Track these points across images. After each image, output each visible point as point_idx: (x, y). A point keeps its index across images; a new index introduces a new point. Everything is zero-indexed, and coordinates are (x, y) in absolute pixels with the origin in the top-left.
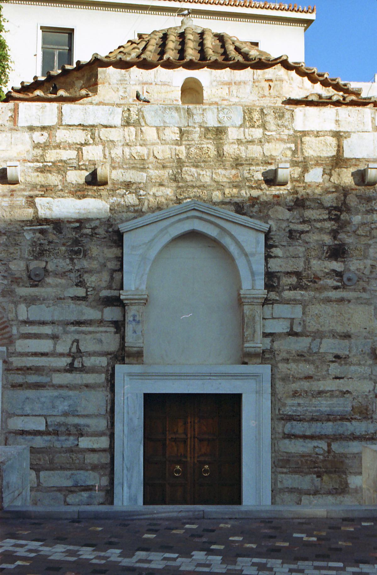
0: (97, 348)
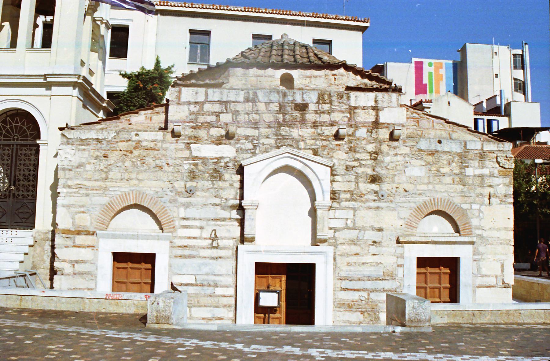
0: (227, 235)
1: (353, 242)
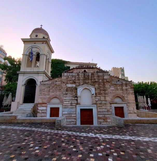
0: (74, 103)
1: (101, 104)
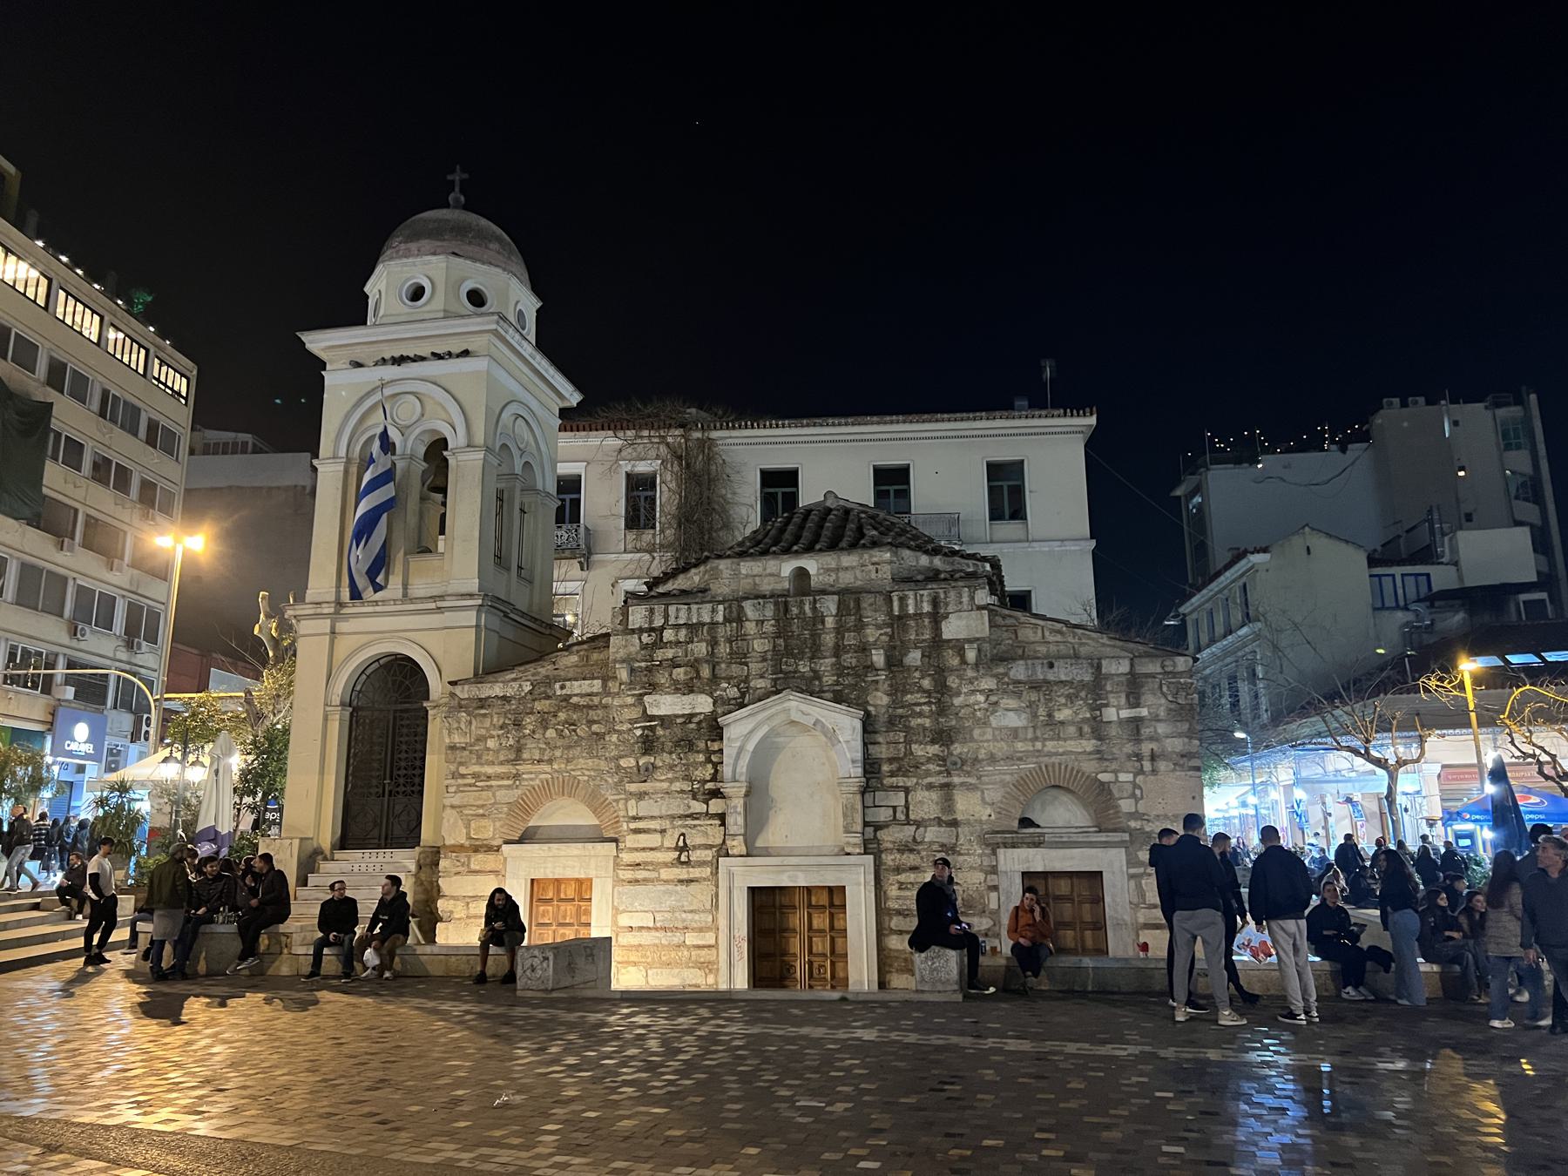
1: (905, 848)
